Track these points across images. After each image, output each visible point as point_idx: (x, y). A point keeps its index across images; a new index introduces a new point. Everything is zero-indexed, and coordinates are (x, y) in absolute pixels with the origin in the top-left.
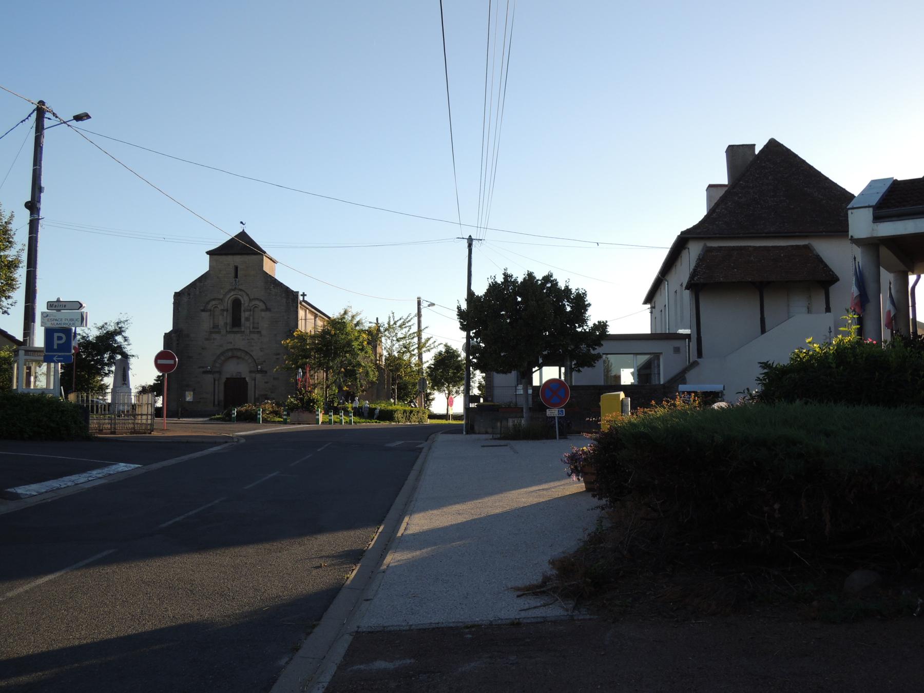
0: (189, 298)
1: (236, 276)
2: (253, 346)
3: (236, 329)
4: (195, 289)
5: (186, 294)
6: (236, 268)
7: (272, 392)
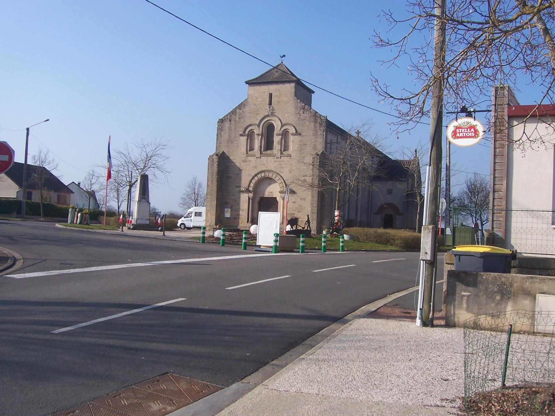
0: (230, 124)
1: (270, 104)
2: (283, 168)
3: (269, 152)
4: (236, 115)
5: (228, 120)
6: (271, 95)
7: (299, 212)
